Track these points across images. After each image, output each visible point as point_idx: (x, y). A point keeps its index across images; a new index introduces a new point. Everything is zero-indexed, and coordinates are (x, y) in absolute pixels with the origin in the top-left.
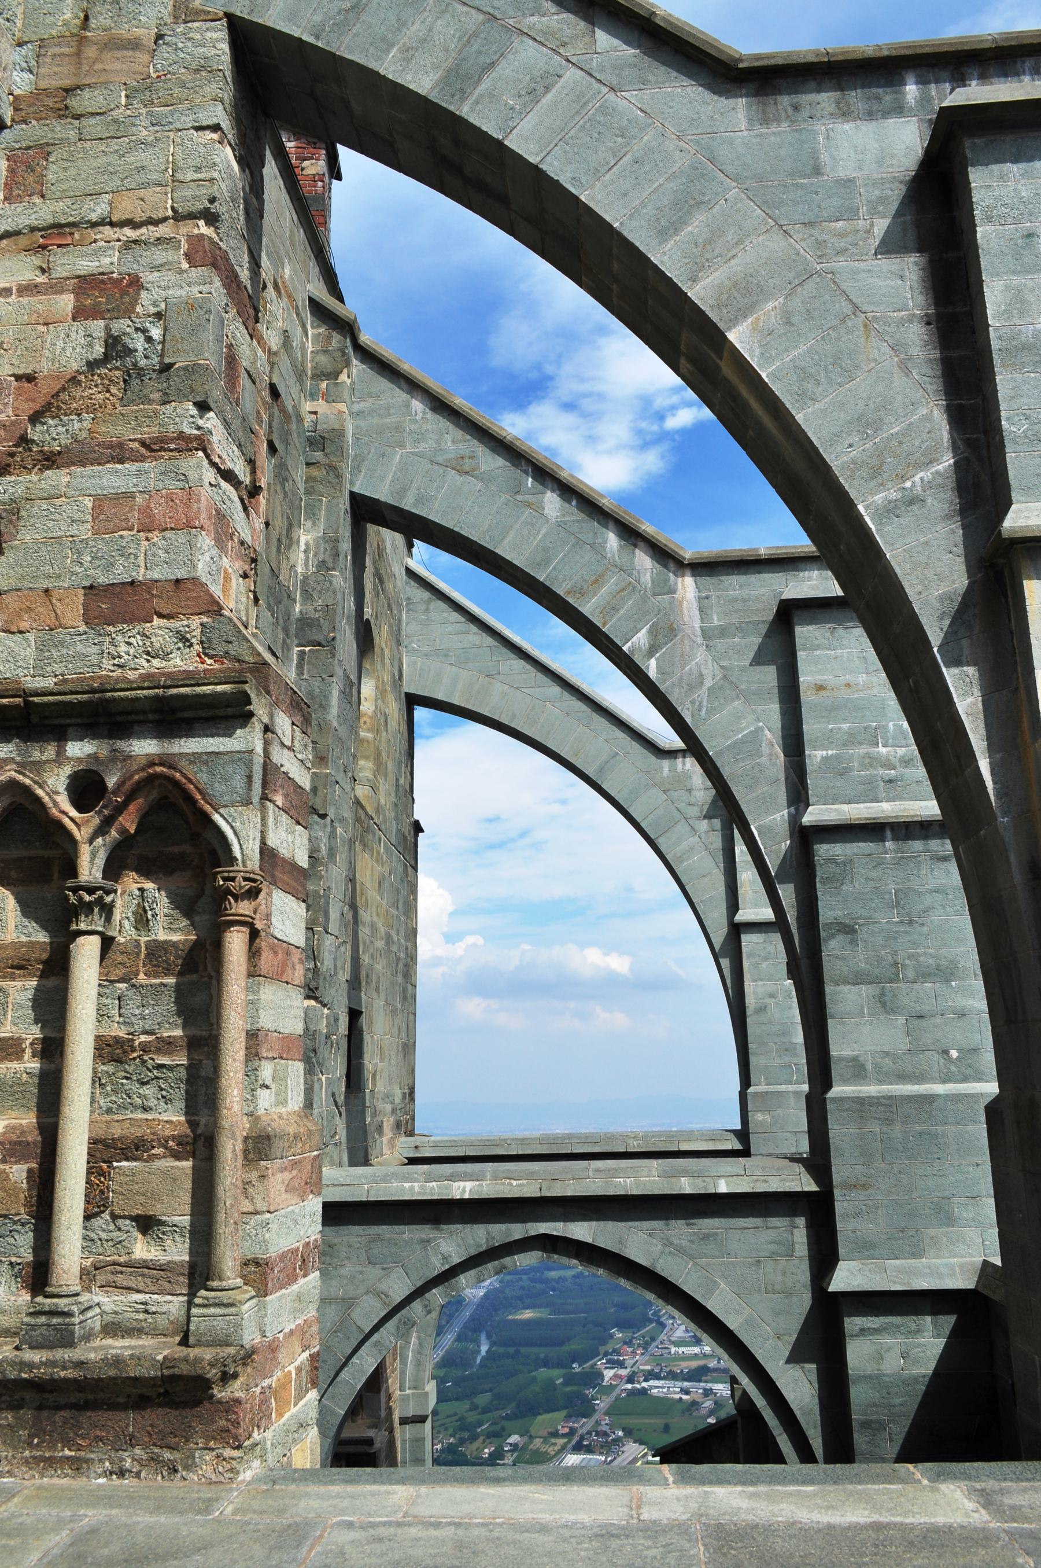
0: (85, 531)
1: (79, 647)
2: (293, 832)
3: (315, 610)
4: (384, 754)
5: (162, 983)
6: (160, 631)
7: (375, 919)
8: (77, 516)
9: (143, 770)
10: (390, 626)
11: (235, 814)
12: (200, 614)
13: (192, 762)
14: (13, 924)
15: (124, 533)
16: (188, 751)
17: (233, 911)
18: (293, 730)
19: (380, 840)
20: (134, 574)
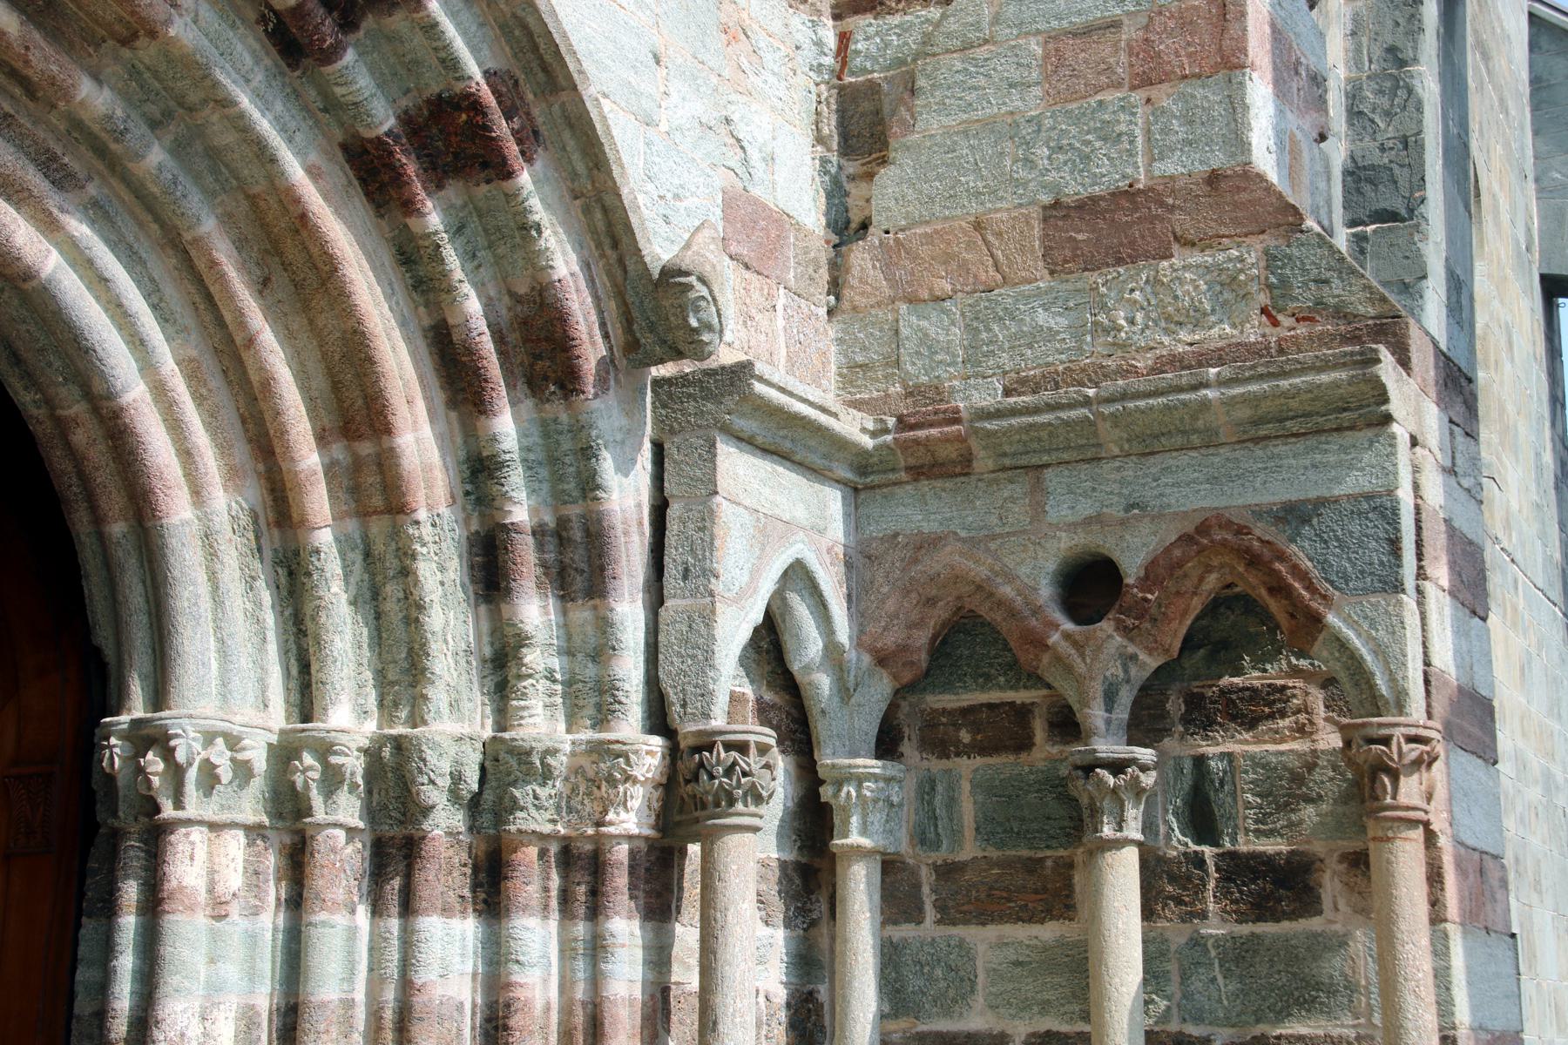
0: (1032, 102)
1: (1042, 317)
2: (1467, 634)
3: (1382, 149)
4: (1510, 408)
5: (1253, 934)
6: (1186, 272)
7: (1520, 744)
8: (1015, 75)
10: (1507, 145)
12: (1263, 232)
15: (1107, 96)
17: (1389, 800)
18: (1452, 433)
19: (1516, 581)
20: (1129, 171)
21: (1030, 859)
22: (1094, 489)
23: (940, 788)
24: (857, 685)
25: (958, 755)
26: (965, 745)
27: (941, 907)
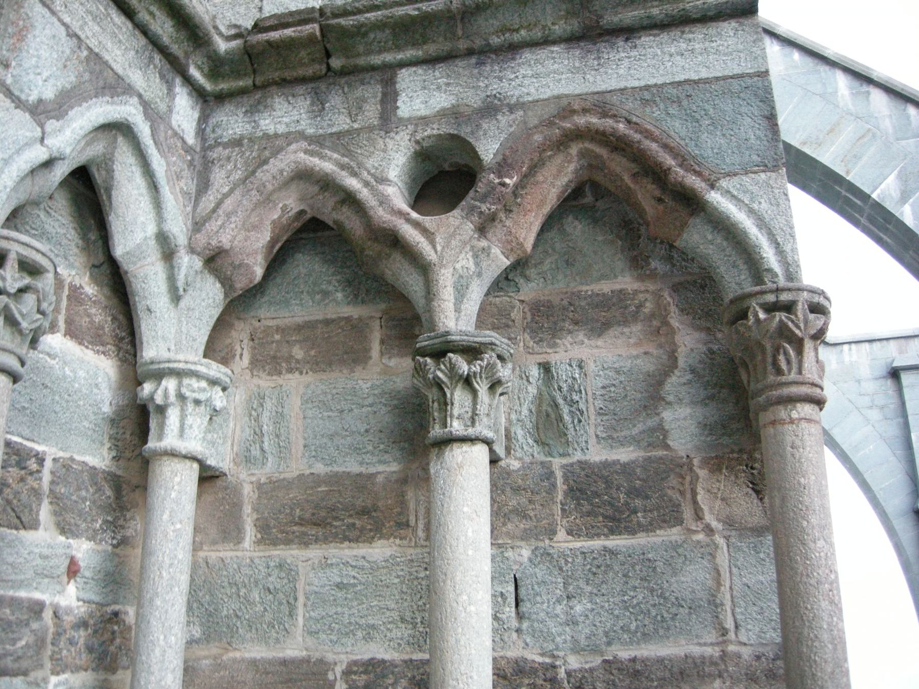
5: (605, 549)
9: (550, 124)
11: (755, 189)
13: (645, 102)
14: (301, 442)
16: (636, 84)
17: (793, 376)
21: (360, 475)
22: (448, 84)
23: (268, 404)
24: (187, 284)
25: (290, 371)
26: (298, 361)
27: (263, 527)
